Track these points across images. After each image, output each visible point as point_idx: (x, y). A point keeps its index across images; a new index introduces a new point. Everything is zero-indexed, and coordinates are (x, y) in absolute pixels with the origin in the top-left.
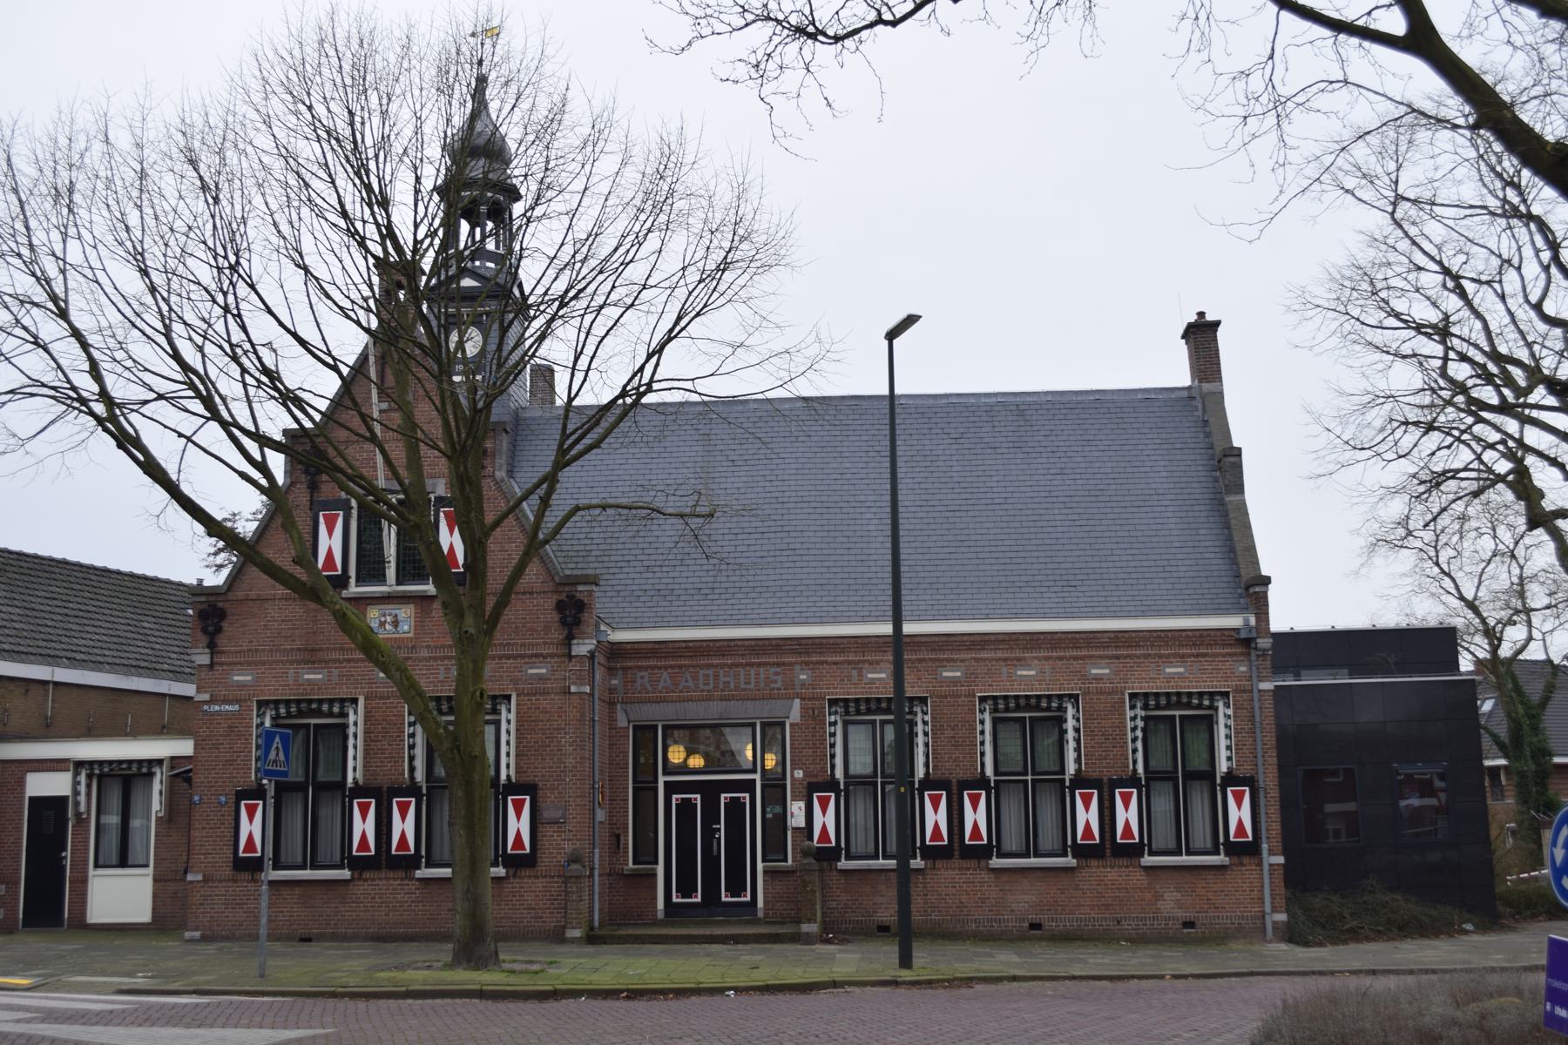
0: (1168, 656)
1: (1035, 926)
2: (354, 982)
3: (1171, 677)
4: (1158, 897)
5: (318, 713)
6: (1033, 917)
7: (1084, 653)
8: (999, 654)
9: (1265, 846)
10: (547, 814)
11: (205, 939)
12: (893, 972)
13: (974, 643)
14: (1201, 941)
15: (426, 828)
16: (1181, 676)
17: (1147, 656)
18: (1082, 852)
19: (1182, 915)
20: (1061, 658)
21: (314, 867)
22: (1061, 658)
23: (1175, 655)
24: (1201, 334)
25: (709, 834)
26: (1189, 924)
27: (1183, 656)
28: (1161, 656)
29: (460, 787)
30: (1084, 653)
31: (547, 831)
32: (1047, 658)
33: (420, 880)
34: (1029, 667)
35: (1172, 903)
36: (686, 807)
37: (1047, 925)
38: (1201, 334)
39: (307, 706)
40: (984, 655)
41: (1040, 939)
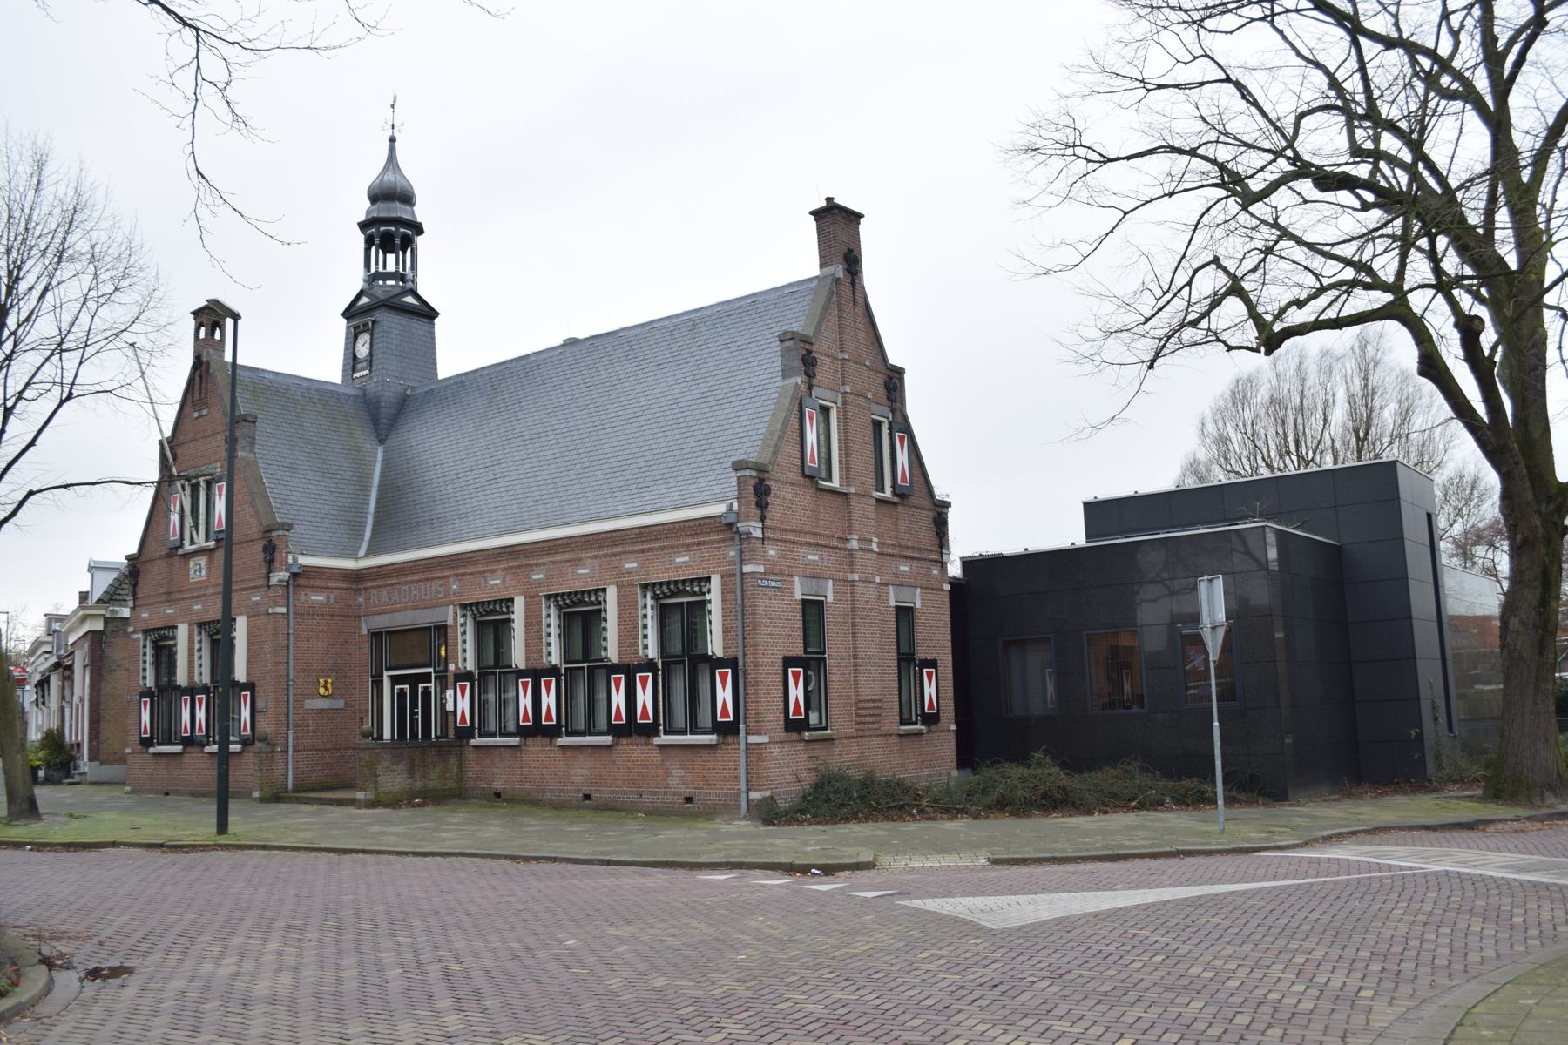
0: (678, 547)
1: (587, 797)
2: (1098, 846)
3: (679, 567)
4: (668, 773)
5: (582, 603)
6: (586, 790)
7: (620, 549)
8: (567, 556)
9: (742, 726)
10: (260, 704)
11: (132, 792)
12: (205, 829)
13: (550, 548)
14: (694, 816)
15: (664, 697)
16: (686, 565)
17: (663, 548)
18: (614, 730)
19: (686, 790)
20: (605, 556)
21: (692, 733)
22: (605, 556)
23: (683, 545)
24: (837, 225)
25: (413, 714)
26: (689, 800)
27: (688, 545)
28: (672, 547)
29: (686, 660)
30: (620, 549)
31: (259, 716)
32: (596, 557)
33: (561, 747)
34: (584, 566)
35: (678, 779)
36: (402, 693)
37: (595, 796)
38: (837, 225)
39: (677, 587)
40: (558, 558)
41: (589, 808)
